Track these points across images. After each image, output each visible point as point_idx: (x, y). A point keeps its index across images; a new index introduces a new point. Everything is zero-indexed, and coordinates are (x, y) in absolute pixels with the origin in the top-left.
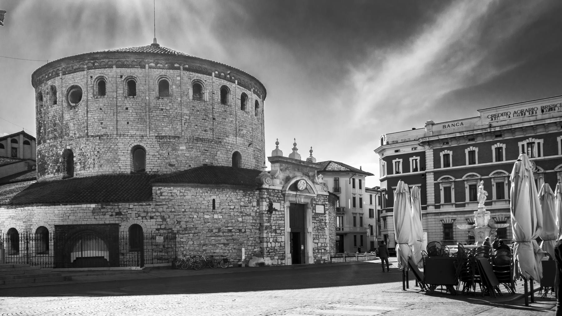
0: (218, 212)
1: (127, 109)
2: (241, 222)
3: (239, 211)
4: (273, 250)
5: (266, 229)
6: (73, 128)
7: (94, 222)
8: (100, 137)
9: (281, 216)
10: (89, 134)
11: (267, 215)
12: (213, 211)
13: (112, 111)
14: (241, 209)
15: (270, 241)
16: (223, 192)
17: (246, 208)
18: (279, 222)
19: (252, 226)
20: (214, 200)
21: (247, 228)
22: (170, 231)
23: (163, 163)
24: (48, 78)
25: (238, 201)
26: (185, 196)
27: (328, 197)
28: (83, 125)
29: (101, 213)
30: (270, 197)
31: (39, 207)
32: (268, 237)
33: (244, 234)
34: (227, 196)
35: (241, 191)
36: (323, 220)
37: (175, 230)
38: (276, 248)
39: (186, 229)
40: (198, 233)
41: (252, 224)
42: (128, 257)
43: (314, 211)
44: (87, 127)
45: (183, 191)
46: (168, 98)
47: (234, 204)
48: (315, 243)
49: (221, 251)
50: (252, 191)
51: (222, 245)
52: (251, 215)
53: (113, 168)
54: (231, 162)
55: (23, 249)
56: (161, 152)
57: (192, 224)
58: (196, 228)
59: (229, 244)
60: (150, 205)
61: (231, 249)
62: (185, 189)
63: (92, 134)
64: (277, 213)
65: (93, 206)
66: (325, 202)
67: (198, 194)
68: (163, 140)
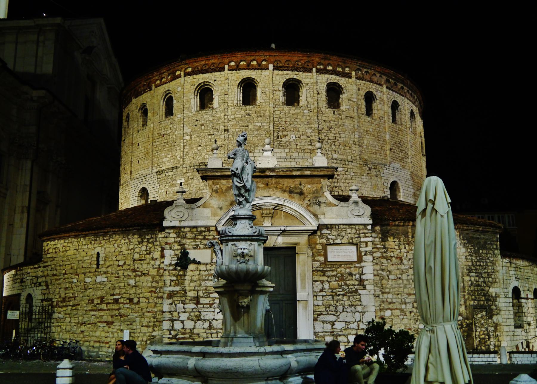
0: (102, 272)
2: (133, 286)
3: (131, 268)
4: (187, 336)
11: (174, 272)
12: (96, 271)
14: (134, 265)
15: (180, 319)
16: (111, 240)
17: (142, 262)
18: (206, 285)
20: (98, 254)
21: (141, 295)
25: (130, 252)
26: (66, 251)
27: (370, 227)
30: (184, 241)
32: (175, 311)
33: (137, 306)
34: (116, 245)
35: (136, 236)
36: (351, 274)
38: (195, 331)
39: (64, 300)
41: (151, 289)
47: (124, 258)
48: (323, 322)
49: (103, 334)
50: (153, 234)
51: (105, 324)
52: (150, 273)
57: (72, 291)
58: (75, 297)
59: (113, 322)
61: (115, 330)
62: (67, 241)
64: (202, 267)
66: (360, 237)
67: (80, 247)
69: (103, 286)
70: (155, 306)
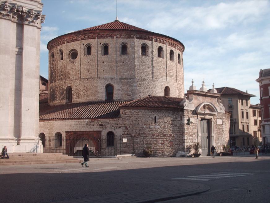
1: (103, 62)
5: (186, 134)
6: (72, 74)
7: (88, 130)
8: (88, 79)
9: (195, 126)
10: (81, 77)
12: (155, 124)
13: (95, 64)
19: (178, 132)
20: (155, 117)
22: (130, 135)
23: (124, 94)
24: (58, 45)
26: (139, 115)
28: (78, 72)
29: (91, 125)
31: (57, 121)
36: (221, 128)
37: (133, 135)
39: (139, 134)
40: (146, 137)
42: (106, 150)
43: (216, 123)
44: (80, 73)
45: (138, 112)
46: (127, 55)
48: (217, 143)
51: (160, 144)
53: (95, 97)
54: (164, 92)
55: (47, 145)
56: (123, 87)
59: (164, 143)
60: (119, 120)
63: (83, 78)
64: (193, 124)
65: (87, 120)
68: (124, 80)
69: (158, 130)
70: (180, 138)
